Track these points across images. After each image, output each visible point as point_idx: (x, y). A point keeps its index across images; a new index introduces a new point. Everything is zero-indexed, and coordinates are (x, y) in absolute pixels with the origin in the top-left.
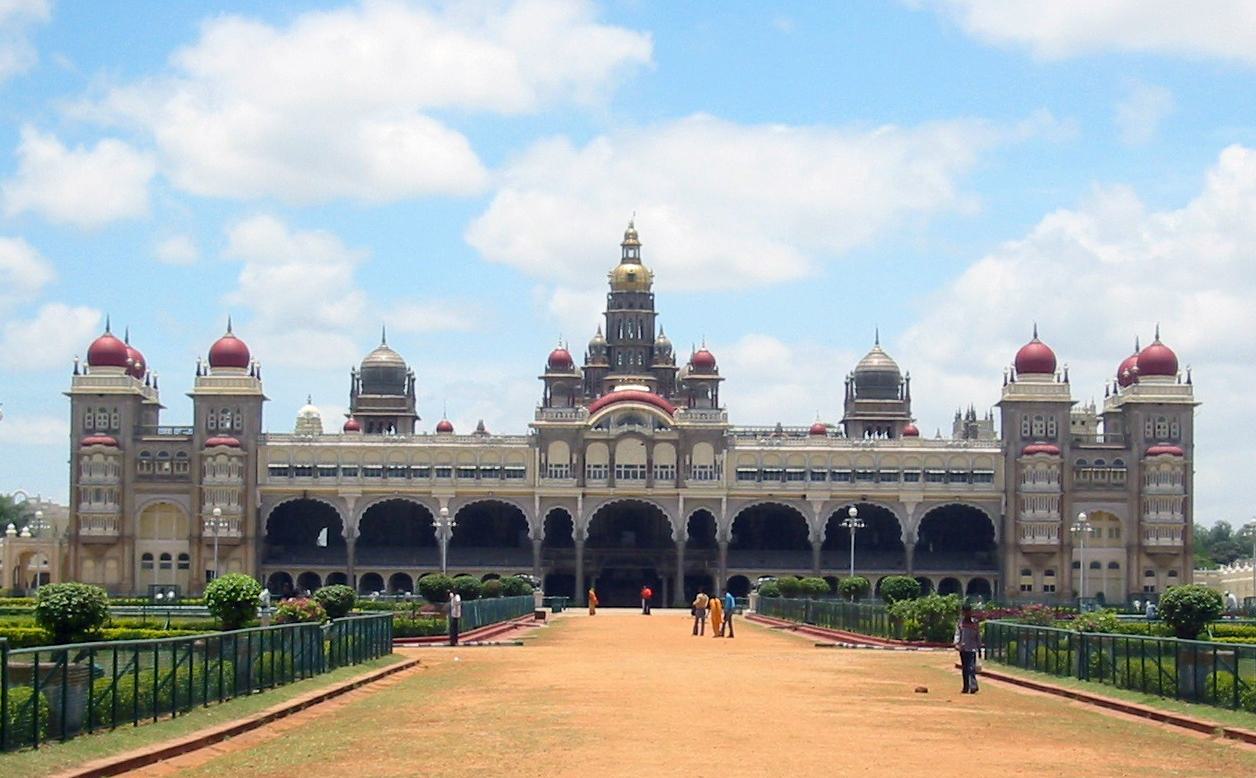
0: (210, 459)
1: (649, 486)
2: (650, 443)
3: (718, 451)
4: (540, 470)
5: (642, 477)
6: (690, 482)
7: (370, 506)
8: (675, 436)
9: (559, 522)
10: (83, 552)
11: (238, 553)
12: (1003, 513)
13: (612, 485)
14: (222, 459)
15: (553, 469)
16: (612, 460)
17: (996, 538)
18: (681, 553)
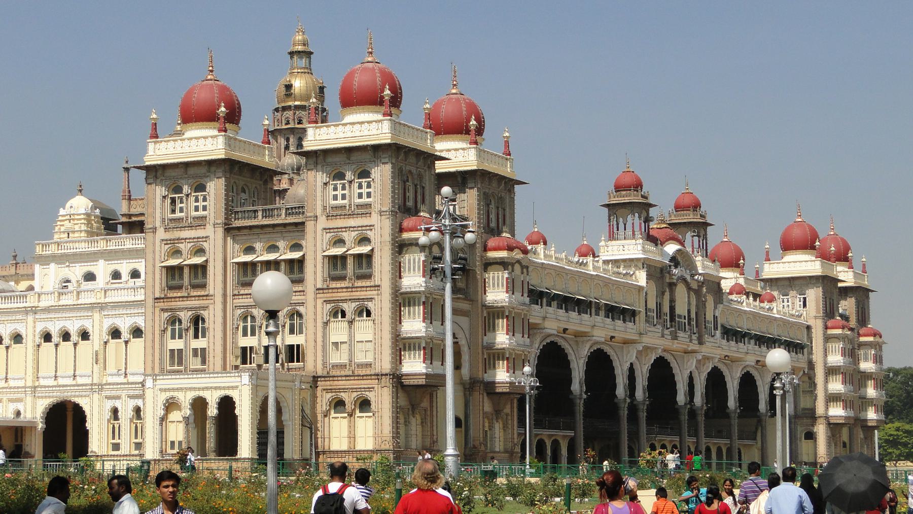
2: (689, 288)
3: (715, 308)
8: (694, 286)
10: (403, 402)
13: (675, 337)
16: (672, 309)
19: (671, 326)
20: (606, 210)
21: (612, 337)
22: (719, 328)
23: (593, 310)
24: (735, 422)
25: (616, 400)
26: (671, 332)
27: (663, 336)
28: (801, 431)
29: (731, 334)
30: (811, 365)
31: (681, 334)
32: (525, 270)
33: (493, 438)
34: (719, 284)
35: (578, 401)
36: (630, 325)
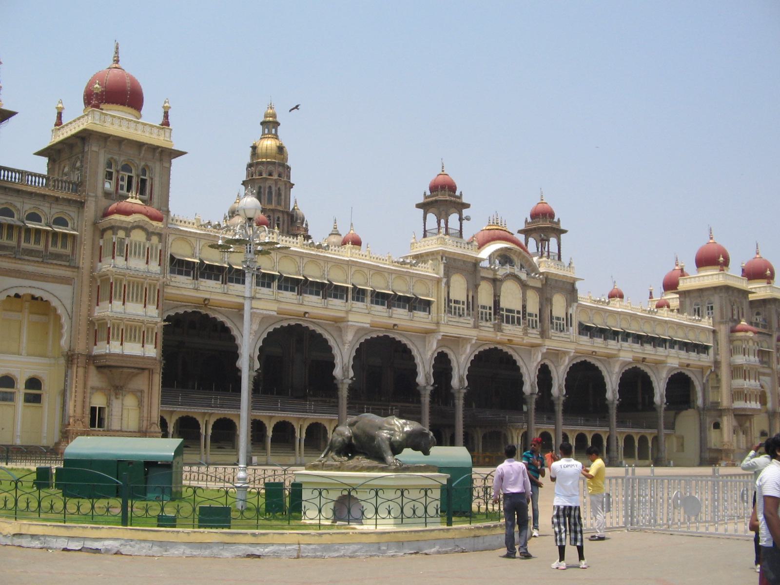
0: (121, 234)
1: (526, 333)
2: (524, 286)
4: (445, 307)
5: (519, 323)
6: (552, 332)
7: (271, 330)
8: (539, 285)
9: (442, 364)
11: (140, 382)
12: (704, 381)
14: (138, 236)
15: (452, 304)
16: (497, 303)
17: (700, 402)
18: (460, 403)
19: (495, 319)
20: (421, 211)
21: (395, 325)
22: (575, 324)
23: (350, 296)
24: (613, 412)
25: (418, 388)
26: (494, 325)
27: (476, 327)
28: (709, 422)
29: (584, 330)
30: (717, 363)
31: (530, 331)
32: (155, 239)
33: (110, 415)
34: (573, 285)
35: (340, 386)
36: (420, 314)
